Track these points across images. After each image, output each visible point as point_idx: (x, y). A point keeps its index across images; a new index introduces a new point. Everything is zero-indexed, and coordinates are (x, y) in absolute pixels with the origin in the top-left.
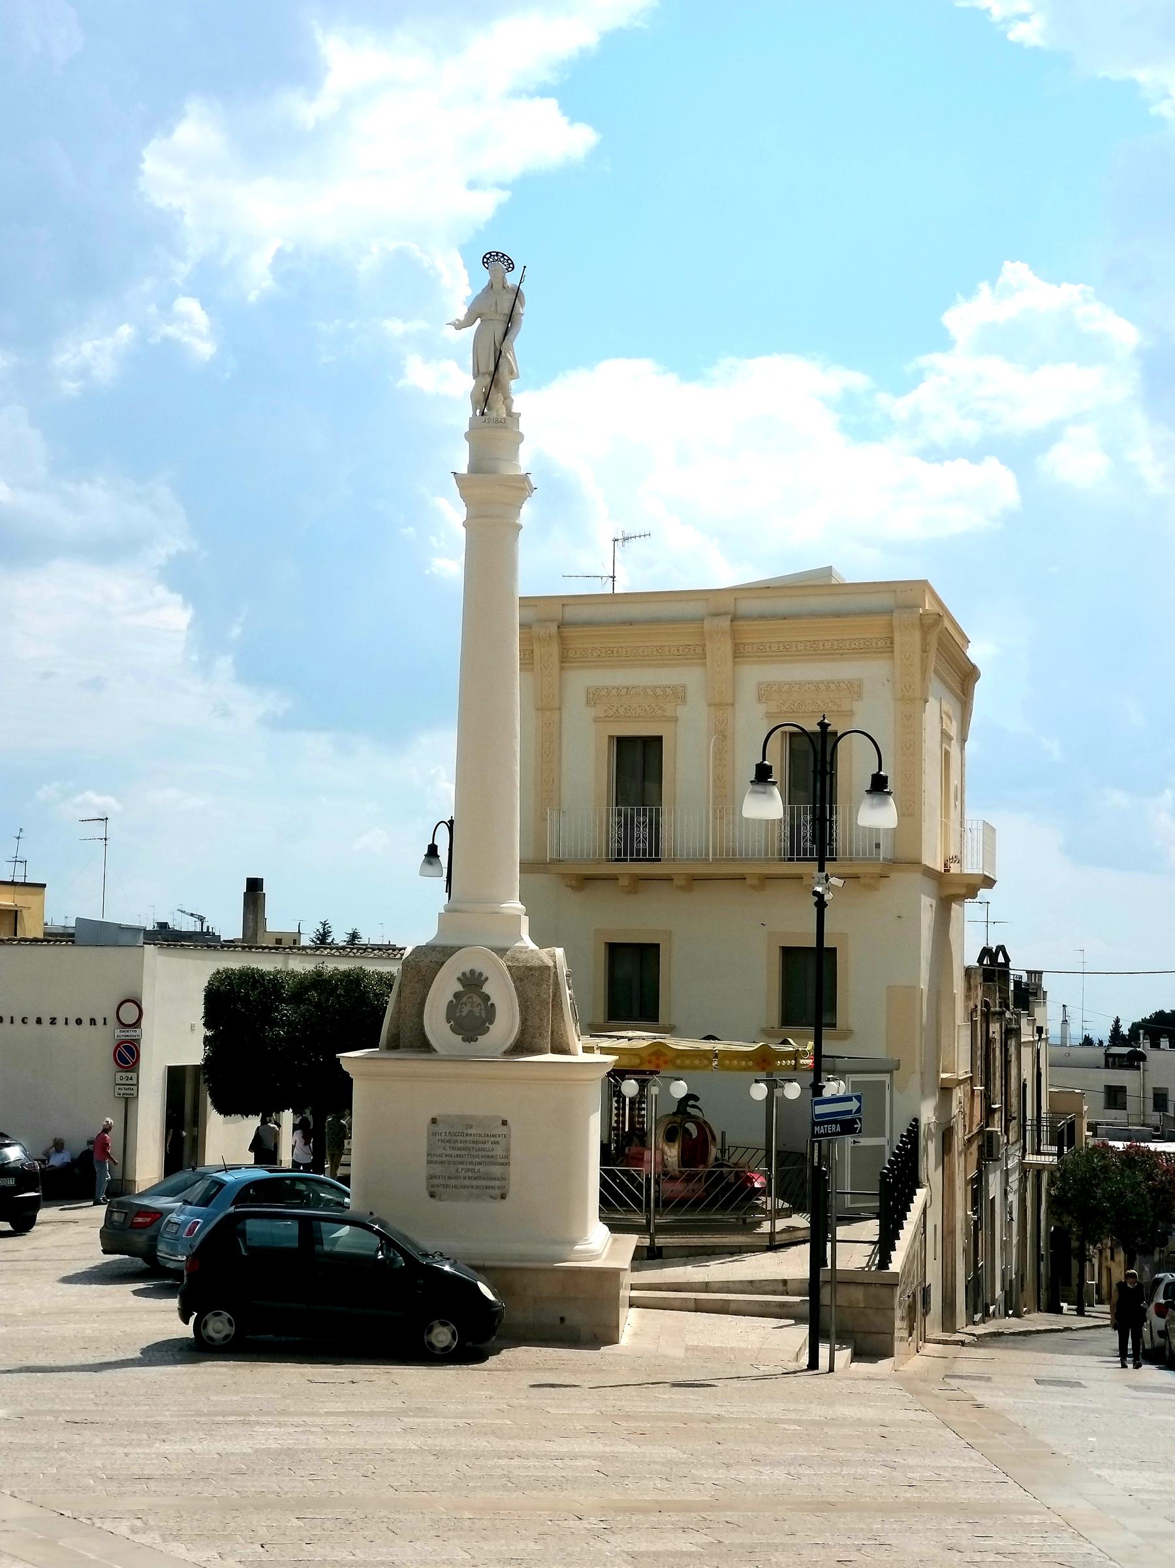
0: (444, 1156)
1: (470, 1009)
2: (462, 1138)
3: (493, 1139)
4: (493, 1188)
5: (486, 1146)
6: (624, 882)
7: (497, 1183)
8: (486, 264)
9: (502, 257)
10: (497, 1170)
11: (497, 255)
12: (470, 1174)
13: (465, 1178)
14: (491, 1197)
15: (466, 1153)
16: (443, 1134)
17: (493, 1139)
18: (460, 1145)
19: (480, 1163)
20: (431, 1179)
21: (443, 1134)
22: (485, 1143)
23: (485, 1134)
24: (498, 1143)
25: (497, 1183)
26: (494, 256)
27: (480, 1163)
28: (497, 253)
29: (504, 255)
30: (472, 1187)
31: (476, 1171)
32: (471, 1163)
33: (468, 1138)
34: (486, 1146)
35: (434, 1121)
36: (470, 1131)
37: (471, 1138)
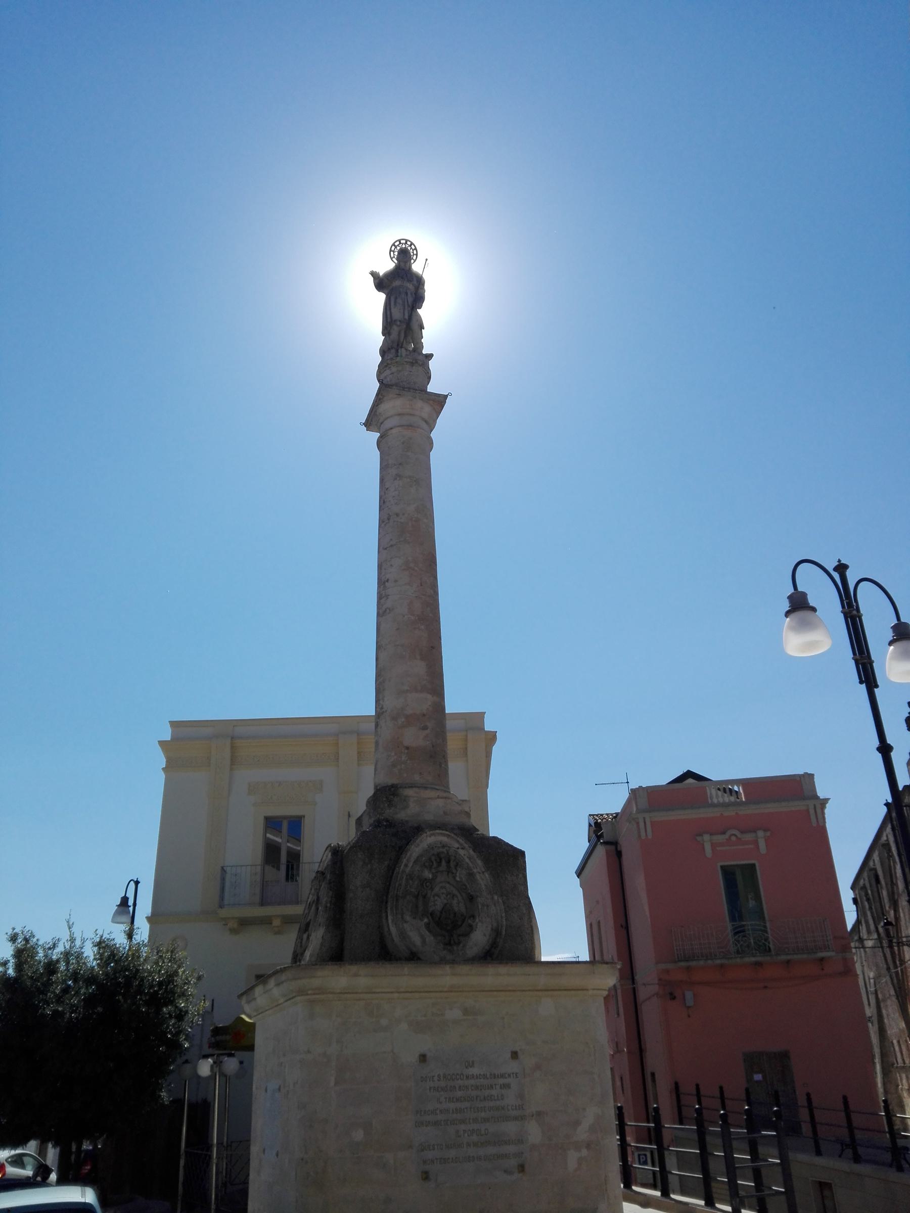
0: (438, 1112)
1: (445, 901)
2: (460, 1082)
3: (501, 1081)
4: (505, 1156)
5: (494, 1092)
6: (277, 922)
7: (511, 1149)
8: (392, 253)
9: (411, 245)
10: (510, 1128)
11: (406, 243)
12: (475, 1138)
13: (469, 1145)
14: (505, 1171)
15: (466, 1104)
16: (436, 1078)
17: (501, 1081)
18: (459, 1094)
19: (486, 1120)
20: (423, 1150)
21: (436, 1078)
22: (492, 1087)
23: (491, 1074)
24: (507, 1086)
25: (511, 1149)
26: (403, 244)
27: (486, 1120)
28: (407, 241)
29: (412, 244)
30: (479, 1158)
31: (483, 1132)
32: (475, 1120)
33: (472, 1082)
34: (494, 1092)
35: (423, 1058)
36: (475, 1071)
37: (472, 1082)
